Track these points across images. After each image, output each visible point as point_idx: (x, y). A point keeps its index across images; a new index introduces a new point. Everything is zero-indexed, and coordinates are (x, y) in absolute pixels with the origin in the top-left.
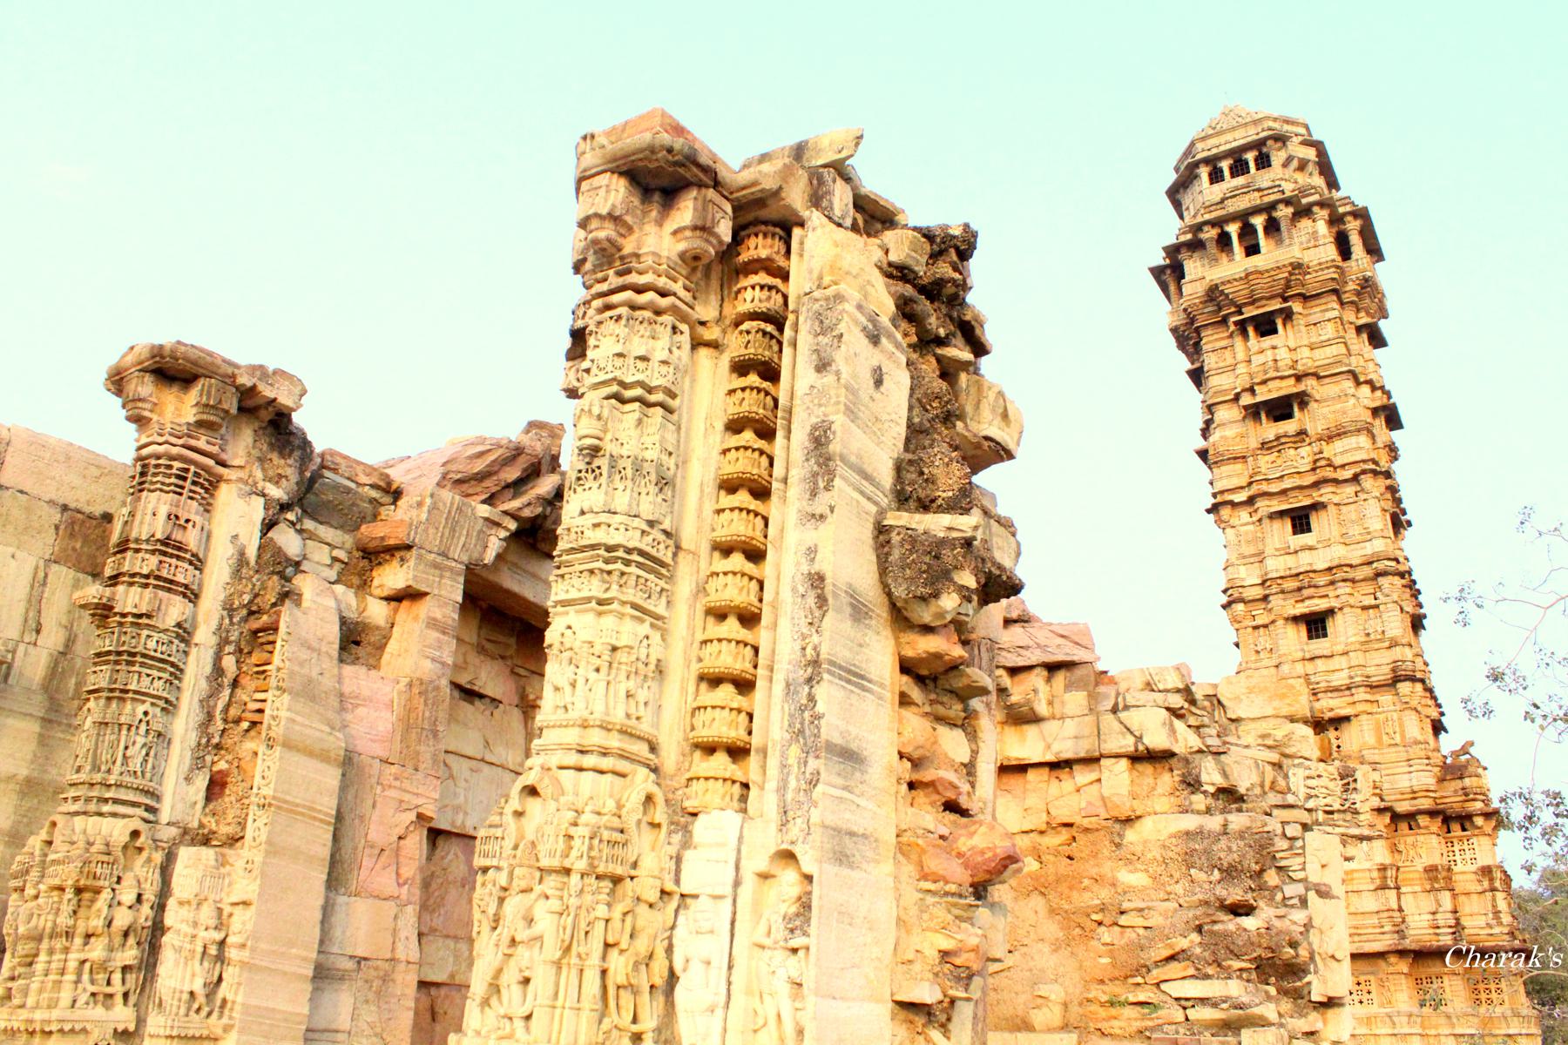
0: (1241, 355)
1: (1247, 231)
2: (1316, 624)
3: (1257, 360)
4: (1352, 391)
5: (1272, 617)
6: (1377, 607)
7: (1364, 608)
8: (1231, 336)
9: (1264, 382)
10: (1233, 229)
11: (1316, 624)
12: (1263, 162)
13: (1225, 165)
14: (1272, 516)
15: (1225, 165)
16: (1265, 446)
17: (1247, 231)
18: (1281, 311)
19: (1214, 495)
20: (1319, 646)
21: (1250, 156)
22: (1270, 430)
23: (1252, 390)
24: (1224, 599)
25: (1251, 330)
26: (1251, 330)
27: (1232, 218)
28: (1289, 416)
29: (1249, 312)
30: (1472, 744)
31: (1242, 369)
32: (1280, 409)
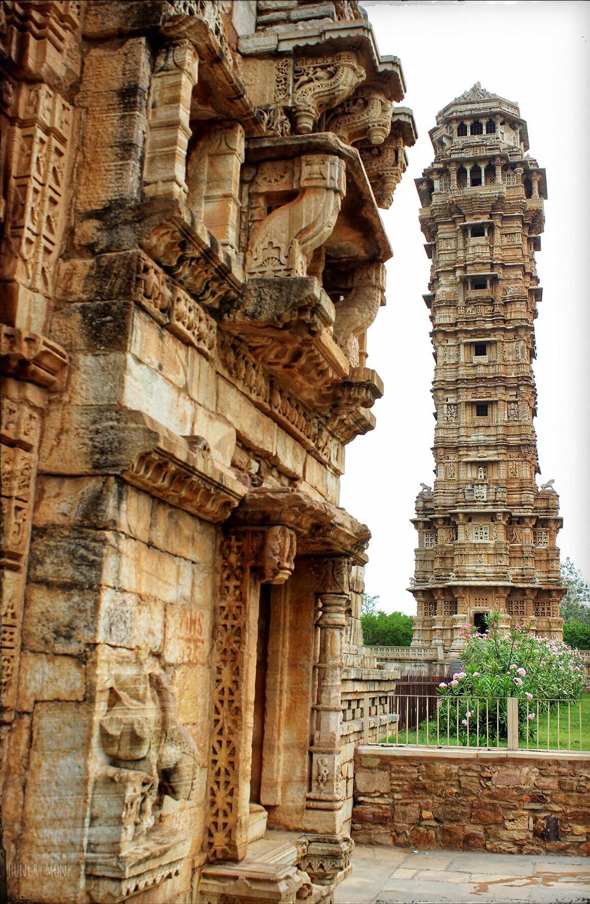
0: (461, 245)
1: (476, 170)
2: (482, 409)
3: (471, 251)
4: (521, 277)
5: (460, 401)
6: (516, 402)
7: (509, 402)
8: (457, 232)
9: (472, 265)
10: (468, 168)
11: (482, 409)
12: (491, 129)
13: (468, 123)
14: (466, 344)
15: (468, 123)
16: (468, 302)
17: (476, 170)
18: (488, 223)
19: (435, 326)
20: (482, 421)
21: (484, 122)
22: (473, 294)
23: (464, 269)
24: (432, 387)
25: (469, 232)
26: (469, 232)
27: (468, 160)
28: (484, 287)
29: (470, 221)
30: (553, 481)
31: (461, 254)
32: (479, 283)
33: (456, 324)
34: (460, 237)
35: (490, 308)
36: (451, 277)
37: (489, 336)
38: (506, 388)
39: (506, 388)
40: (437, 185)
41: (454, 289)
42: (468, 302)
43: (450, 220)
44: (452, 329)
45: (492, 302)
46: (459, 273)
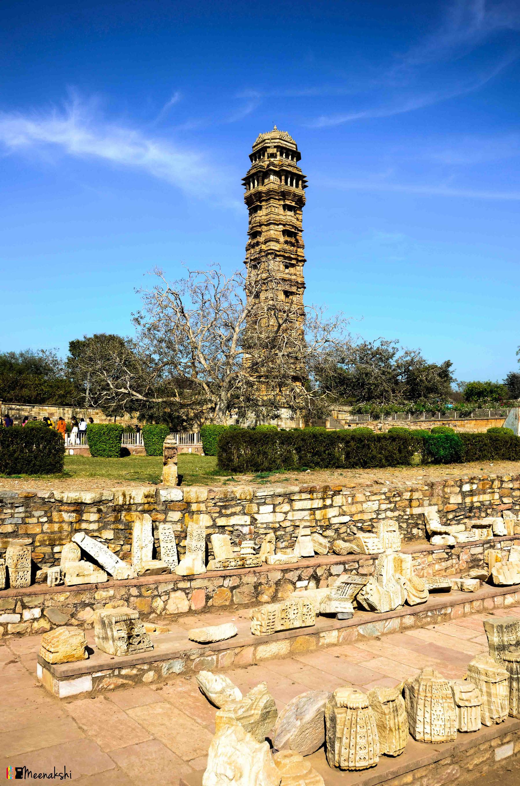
6: (299, 294)
8: (280, 205)
11: (287, 294)
16: (286, 242)
22: (289, 239)
23: (284, 225)
29: (288, 202)
33: (279, 251)
34: (281, 208)
35: (293, 248)
36: (276, 227)
37: (291, 261)
38: (298, 288)
39: (298, 288)
40: (272, 177)
41: (279, 233)
42: (286, 242)
43: (277, 198)
44: (278, 253)
45: (293, 245)
46: (281, 227)
